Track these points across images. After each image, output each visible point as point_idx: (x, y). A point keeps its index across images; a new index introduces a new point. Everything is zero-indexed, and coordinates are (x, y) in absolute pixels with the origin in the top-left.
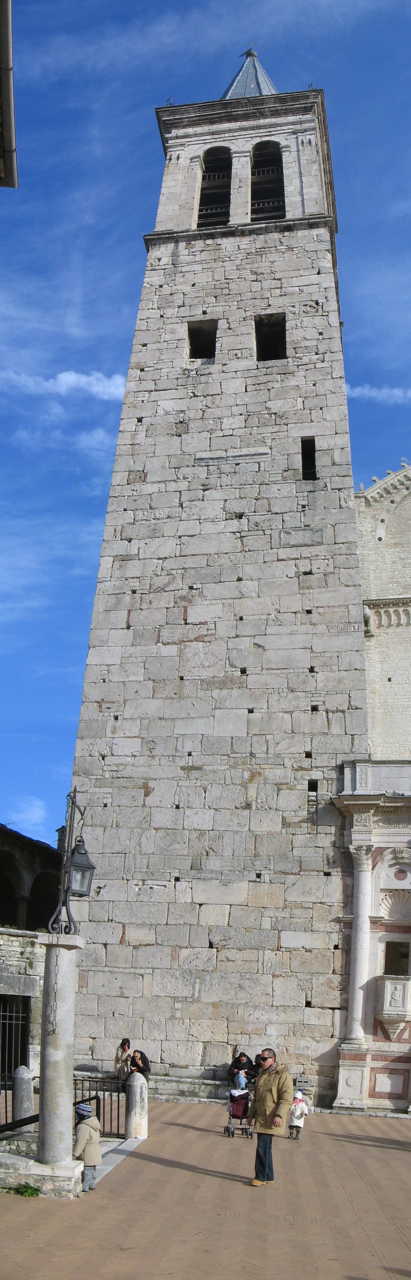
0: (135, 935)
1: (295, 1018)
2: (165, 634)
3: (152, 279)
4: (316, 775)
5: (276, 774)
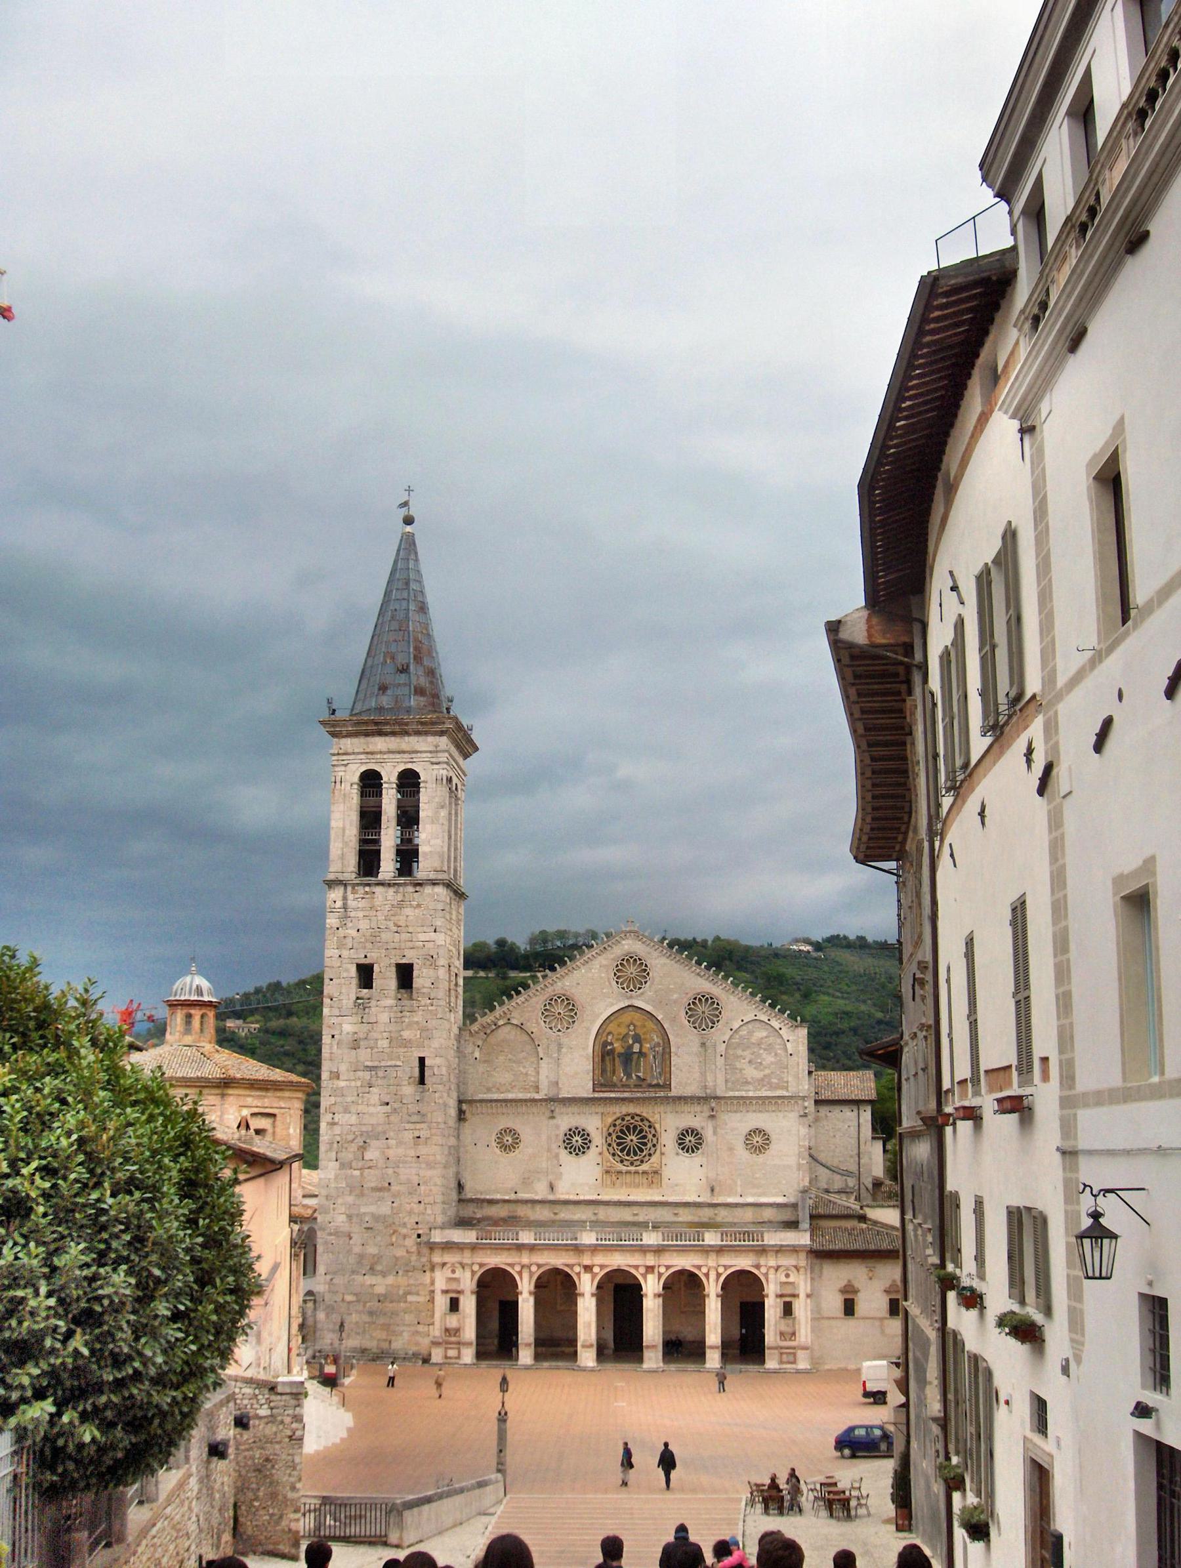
0: (349, 1298)
1: (413, 1329)
2: (354, 1164)
3: (332, 921)
4: (420, 1232)
5: (404, 1231)
